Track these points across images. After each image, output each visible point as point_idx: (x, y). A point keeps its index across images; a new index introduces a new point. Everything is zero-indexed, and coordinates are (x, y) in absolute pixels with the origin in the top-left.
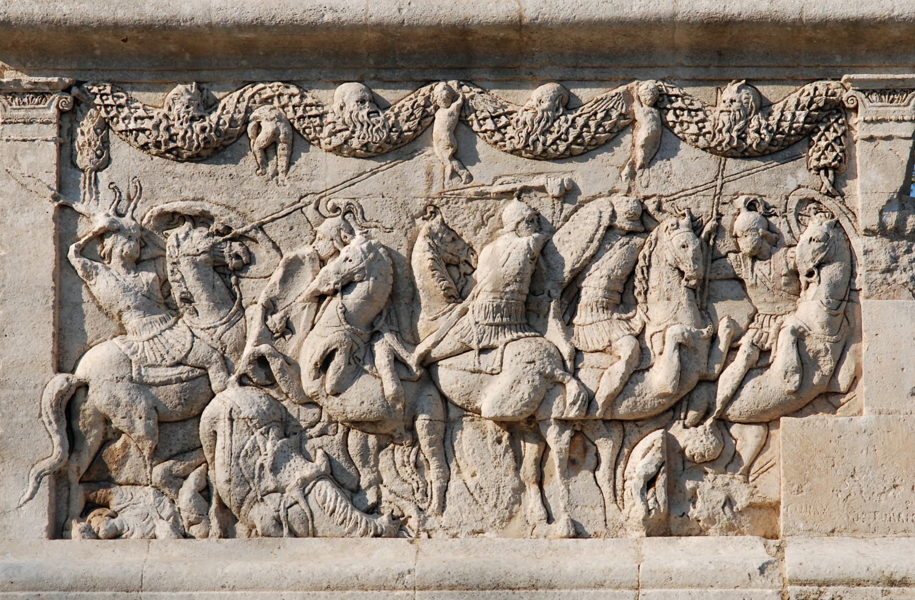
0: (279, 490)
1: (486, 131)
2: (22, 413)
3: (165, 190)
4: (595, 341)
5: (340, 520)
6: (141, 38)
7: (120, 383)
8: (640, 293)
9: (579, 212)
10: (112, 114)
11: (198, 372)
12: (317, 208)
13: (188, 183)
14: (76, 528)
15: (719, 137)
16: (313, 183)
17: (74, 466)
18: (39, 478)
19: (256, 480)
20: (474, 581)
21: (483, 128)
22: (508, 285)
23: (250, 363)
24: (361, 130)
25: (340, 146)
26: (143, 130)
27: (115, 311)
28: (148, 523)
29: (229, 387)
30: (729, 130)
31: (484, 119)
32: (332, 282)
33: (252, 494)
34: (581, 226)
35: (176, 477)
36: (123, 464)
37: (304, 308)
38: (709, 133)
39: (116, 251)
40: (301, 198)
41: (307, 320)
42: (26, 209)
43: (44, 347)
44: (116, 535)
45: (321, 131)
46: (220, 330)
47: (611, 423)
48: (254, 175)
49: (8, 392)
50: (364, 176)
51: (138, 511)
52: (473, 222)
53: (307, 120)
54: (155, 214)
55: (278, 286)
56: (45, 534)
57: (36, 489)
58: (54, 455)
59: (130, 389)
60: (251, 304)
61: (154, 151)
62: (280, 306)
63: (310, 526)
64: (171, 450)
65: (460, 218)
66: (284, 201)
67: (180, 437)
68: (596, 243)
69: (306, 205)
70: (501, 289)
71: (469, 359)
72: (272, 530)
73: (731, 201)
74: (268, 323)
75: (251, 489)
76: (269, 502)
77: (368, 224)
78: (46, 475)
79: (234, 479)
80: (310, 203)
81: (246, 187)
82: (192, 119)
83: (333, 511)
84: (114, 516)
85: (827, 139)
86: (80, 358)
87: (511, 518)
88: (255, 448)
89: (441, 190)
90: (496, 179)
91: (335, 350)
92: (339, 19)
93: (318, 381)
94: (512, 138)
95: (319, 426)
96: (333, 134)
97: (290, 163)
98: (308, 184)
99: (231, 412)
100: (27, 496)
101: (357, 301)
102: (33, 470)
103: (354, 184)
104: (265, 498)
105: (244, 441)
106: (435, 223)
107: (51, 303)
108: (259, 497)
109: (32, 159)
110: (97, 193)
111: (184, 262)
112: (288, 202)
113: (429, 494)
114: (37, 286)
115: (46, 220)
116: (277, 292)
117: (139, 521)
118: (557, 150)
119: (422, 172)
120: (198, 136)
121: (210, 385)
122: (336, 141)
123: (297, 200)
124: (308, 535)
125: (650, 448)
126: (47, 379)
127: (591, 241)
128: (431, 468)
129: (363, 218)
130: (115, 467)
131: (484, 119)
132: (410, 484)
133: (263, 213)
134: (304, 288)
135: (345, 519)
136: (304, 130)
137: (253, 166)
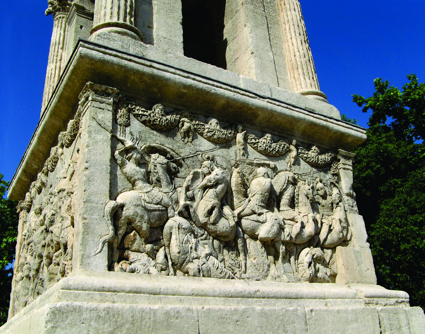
0: (198, 258)
1: (252, 143)
2: (96, 214)
3: (150, 139)
4: (288, 216)
5: (220, 272)
6: (148, 82)
7: (138, 207)
8: (296, 203)
9: (278, 174)
10: (133, 107)
11: (164, 208)
12: (202, 156)
13: (158, 138)
14: (117, 267)
15: (312, 159)
16: (200, 148)
17: (116, 241)
18: (104, 243)
19: (190, 253)
20: (279, 296)
21: (251, 142)
22: (265, 193)
23: (183, 208)
24: (218, 133)
25: (210, 137)
26: (145, 115)
27: (133, 179)
28: (146, 268)
29: (175, 216)
30: (315, 158)
31: (252, 139)
32: (212, 182)
33: (188, 259)
34: (281, 179)
35: (155, 250)
36: (134, 242)
37: (199, 191)
38: (310, 157)
39: (134, 156)
40: (197, 152)
41: (200, 196)
42: (100, 133)
43: (106, 188)
44: (133, 271)
45: (204, 131)
46: (171, 194)
47: (295, 244)
48: (181, 141)
49: (91, 204)
50: (216, 149)
51: (141, 262)
52: (249, 172)
53: (199, 126)
54: (147, 146)
55: (190, 181)
56: (107, 268)
57: (103, 247)
58: (110, 234)
59: (142, 210)
60: (179, 187)
61: (148, 124)
62: (190, 189)
63: (209, 273)
64: (152, 239)
65: (245, 169)
66: (191, 152)
67: (156, 234)
68: (286, 184)
69: (198, 155)
70: (264, 193)
71: (254, 217)
72: (197, 274)
73: (315, 179)
74: (187, 194)
75: (187, 257)
76: (195, 262)
77: (218, 165)
78: (106, 242)
79: (181, 252)
80: (200, 154)
81: (178, 144)
82: (163, 115)
83: (218, 268)
84: (131, 264)
85: (335, 166)
86: (117, 196)
87: (267, 276)
88: (188, 241)
89: (239, 159)
90: (255, 159)
91: (215, 206)
92: (216, 93)
93: (208, 218)
94: (260, 146)
95: (204, 236)
96: (208, 132)
97: (193, 140)
98: (199, 148)
99: (179, 225)
100: (99, 250)
101: (220, 190)
102: (101, 240)
103: (213, 151)
104: (193, 260)
105: (183, 238)
106: (238, 169)
107: (109, 171)
108: (191, 260)
109: (103, 115)
110: (125, 134)
111: (158, 166)
112: (192, 153)
113: (241, 265)
114: (103, 163)
115: (108, 139)
116: (190, 183)
117: (142, 267)
118: (272, 153)
119: (233, 152)
120: (165, 121)
121: (167, 214)
122: (209, 134)
123: (195, 152)
124: (208, 277)
125: (308, 253)
126: (107, 202)
127: (284, 184)
128: (241, 255)
129: (217, 163)
130: (130, 243)
131: (252, 139)
132: (234, 261)
133: (184, 154)
134: (199, 183)
135: (222, 271)
136: (198, 128)
137: (180, 137)
